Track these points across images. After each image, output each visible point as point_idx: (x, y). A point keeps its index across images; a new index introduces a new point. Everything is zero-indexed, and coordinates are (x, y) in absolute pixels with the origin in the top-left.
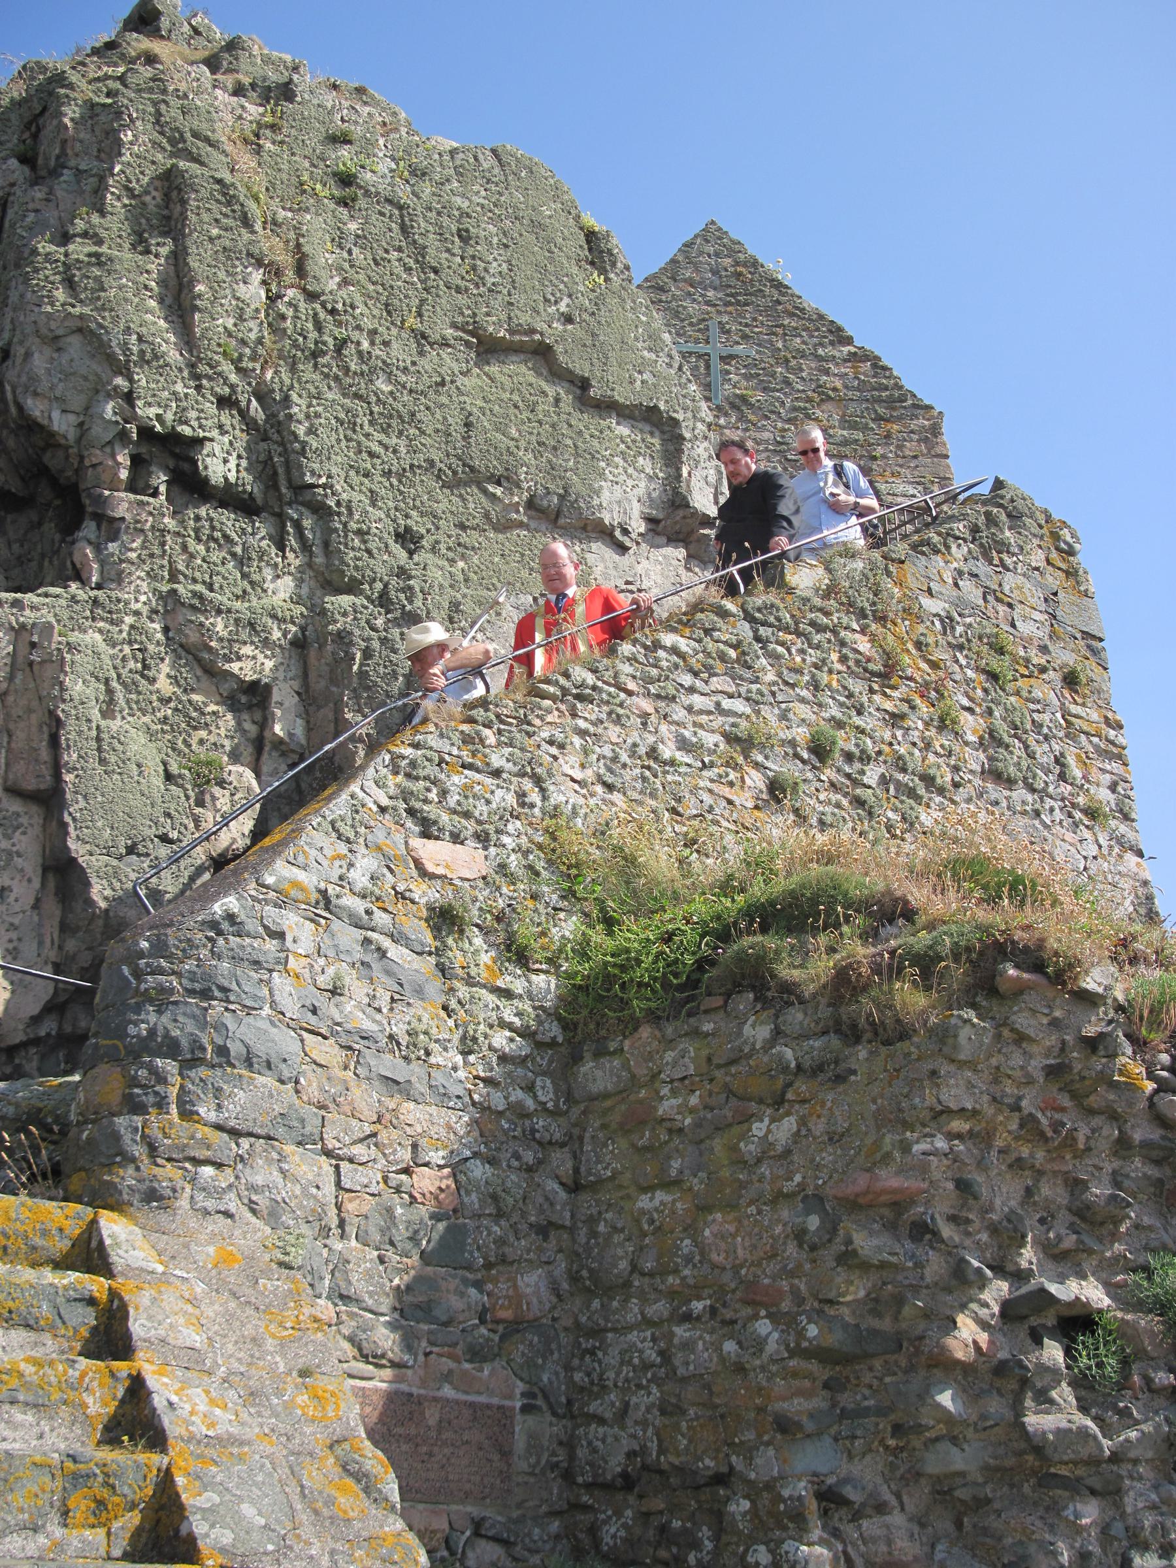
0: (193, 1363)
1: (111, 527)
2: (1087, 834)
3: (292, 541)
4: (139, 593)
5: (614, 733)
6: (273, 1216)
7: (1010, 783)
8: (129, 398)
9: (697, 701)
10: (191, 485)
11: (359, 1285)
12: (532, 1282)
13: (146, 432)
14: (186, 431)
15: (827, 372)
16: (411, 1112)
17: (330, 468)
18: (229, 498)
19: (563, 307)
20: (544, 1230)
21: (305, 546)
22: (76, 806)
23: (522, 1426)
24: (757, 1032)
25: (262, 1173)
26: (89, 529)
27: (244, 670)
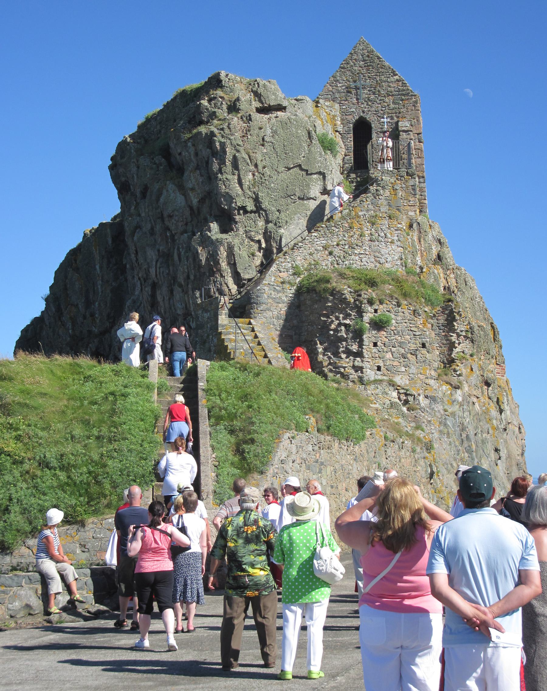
0: (260, 332)
1: (236, 223)
2: (390, 246)
3: (261, 216)
4: (241, 231)
5: (305, 251)
6: (266, 318)
7: (374, 241)
8: (236, 202)
9: (318, 243)
10: (246, 212)
11: (275, 323)
12: (295, 322)
13: (239, 207)
14: (244, 205)
15: (390, 87)
16: (280, 305)
17: (265, 204)
18: (251, 212)
19: (303, 155)
20: (296, 316)
21: (263, 217)
22: (238, 265)
23: (294, 337)
24: (315, 295)
25: (265, 314)
26: (233, 222)
27: (257, 239)
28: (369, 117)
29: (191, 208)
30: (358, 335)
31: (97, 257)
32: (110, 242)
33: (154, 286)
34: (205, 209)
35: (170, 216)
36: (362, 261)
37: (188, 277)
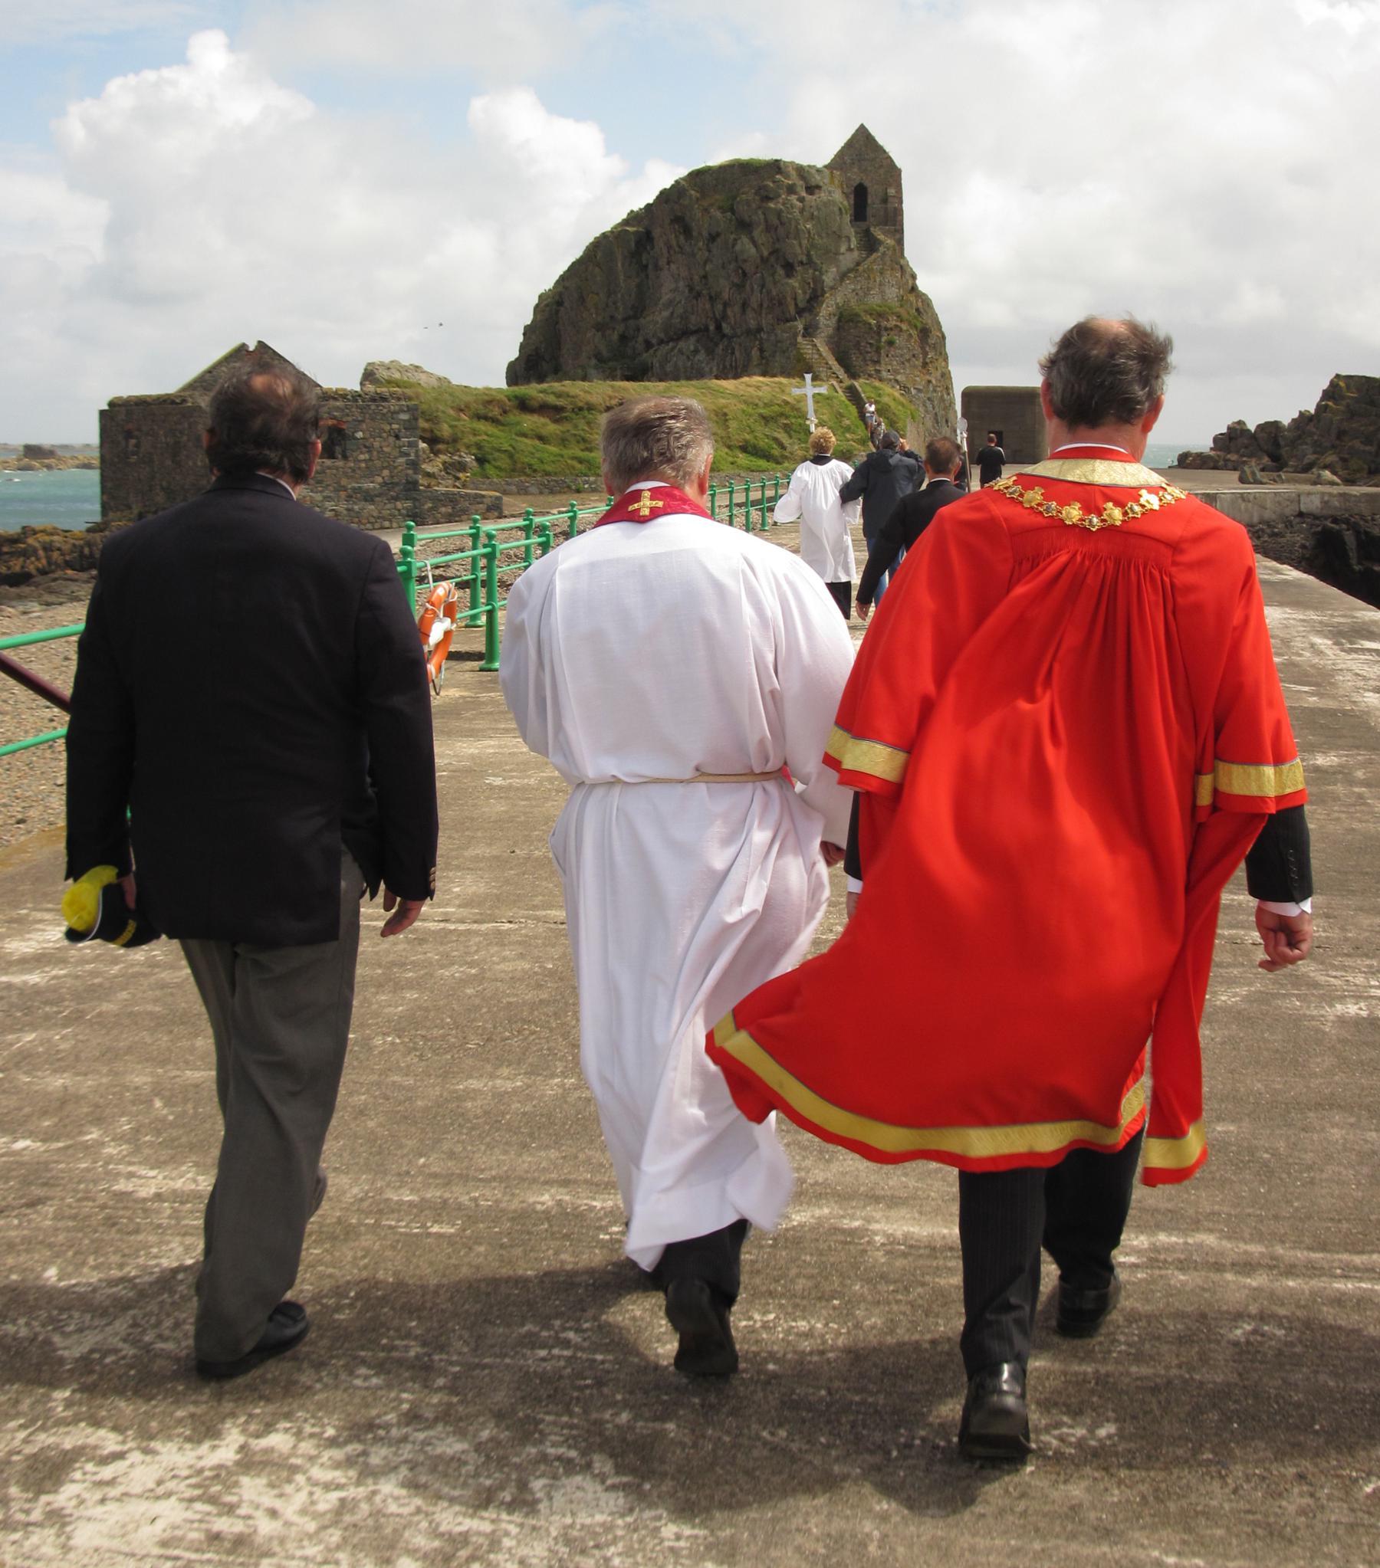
17: (815, 259)
28: (867, 183)
29: (762, 257)
30: (878, 350)
31: (620, 257)
32: (633, 244)
33: (725, 305)
34: (772, 259)
35: (745, 261)
36: (874, 300)
37: (761, 305)
